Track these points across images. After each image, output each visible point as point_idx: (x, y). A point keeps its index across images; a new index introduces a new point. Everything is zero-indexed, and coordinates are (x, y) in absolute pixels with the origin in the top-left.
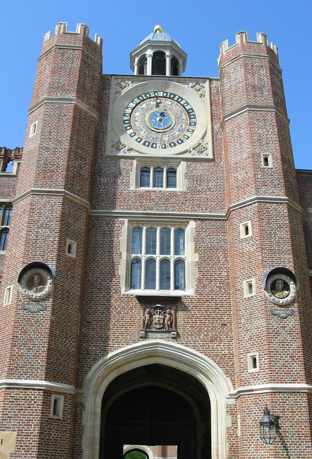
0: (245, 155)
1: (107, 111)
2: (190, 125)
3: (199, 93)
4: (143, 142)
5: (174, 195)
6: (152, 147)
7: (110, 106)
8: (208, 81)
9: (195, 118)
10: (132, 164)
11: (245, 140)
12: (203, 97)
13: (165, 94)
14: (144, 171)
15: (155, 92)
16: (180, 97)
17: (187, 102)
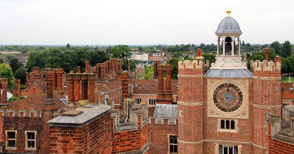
0: (260, 128)
1: (207, 96)
2: (240, 100)
3: (244, 85)
4: (221, 108)
5: (233, 134)
6: (225, 111)
7: (208, 95)
8: (248, 79)
9: (242, 97)
10: (217, 120)
11: (260, 120)
12: (245, 88)
13: (230, 85)
14: (222, 122)
15: (225, 84)
16: (236, 86)
17: (239, 89)
